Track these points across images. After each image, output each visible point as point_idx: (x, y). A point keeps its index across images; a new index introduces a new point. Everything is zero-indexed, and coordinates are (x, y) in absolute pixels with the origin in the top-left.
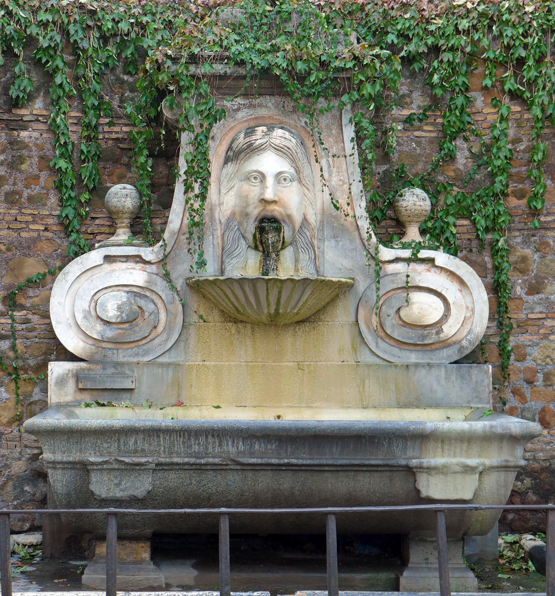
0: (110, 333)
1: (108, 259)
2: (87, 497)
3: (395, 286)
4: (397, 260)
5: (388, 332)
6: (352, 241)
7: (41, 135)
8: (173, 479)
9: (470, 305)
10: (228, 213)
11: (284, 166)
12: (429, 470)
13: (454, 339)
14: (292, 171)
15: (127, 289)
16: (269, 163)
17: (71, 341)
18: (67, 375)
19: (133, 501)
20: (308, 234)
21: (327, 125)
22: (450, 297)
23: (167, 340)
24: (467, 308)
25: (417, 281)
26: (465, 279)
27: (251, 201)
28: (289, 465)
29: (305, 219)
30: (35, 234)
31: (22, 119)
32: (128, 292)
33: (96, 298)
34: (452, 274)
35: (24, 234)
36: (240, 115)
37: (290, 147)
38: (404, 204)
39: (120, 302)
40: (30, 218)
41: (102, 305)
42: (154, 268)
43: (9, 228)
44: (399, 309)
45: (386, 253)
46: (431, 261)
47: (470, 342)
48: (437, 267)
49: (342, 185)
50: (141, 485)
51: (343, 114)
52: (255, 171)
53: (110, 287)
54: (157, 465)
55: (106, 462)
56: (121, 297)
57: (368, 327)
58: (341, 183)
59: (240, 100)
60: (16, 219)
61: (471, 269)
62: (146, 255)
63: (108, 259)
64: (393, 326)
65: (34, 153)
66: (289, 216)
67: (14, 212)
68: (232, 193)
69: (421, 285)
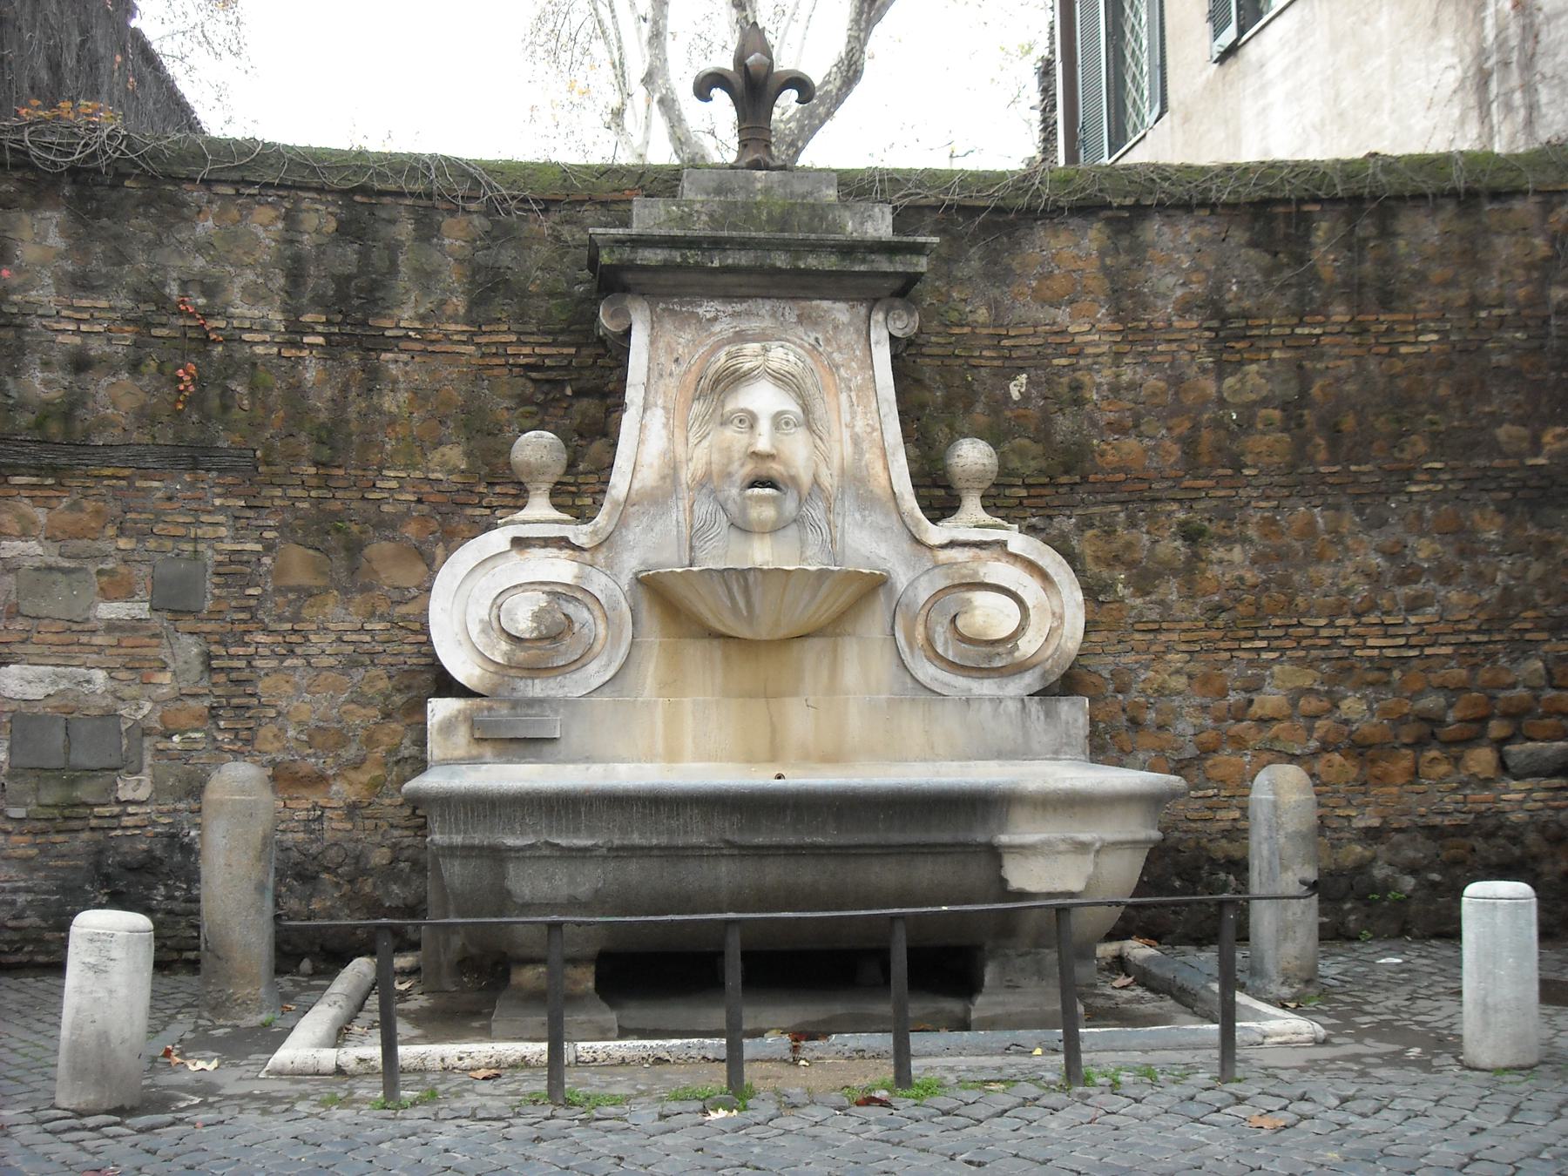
0: (521, 655)
1: (519, 543)
2: (503, 900)
3: (948, 583)
4: (952, 544)
5: (940, 650)
6: (887, 515)
8: (634, 871)
9: (1057, 610)
11: (788, 404)
12: (1021, 849)
13: (1035, 660)
14: (797, 410)
15: (547, 588)
16: (763, 399)
17: (462, 668)
19: (573, 904)
21: (848, 344)
22: (1030, 597)
24: (1054, 614)
26: (1051, 571)
27: (736, 456)
28: (814, 846)
29: (816, 481)
30: (403, 508)
32: (549, 593)
33: (499, 601)
34: (1032, 567)
36: (717, 328)
38: (961, 462)
39: (536, 608)
40: (394, 484)
41: (509, 612)
42: (587, 555)
43: (363, 498)
45: (936, 534)
46: (1003, 544)
50: (587, 880)
52: (742, 410)
54: (609, 849)
55: (531, 846)
62: (576, 536)
63: (519, 543)
64: (946, 643)
66: (794, 480)
68: (705, 443)
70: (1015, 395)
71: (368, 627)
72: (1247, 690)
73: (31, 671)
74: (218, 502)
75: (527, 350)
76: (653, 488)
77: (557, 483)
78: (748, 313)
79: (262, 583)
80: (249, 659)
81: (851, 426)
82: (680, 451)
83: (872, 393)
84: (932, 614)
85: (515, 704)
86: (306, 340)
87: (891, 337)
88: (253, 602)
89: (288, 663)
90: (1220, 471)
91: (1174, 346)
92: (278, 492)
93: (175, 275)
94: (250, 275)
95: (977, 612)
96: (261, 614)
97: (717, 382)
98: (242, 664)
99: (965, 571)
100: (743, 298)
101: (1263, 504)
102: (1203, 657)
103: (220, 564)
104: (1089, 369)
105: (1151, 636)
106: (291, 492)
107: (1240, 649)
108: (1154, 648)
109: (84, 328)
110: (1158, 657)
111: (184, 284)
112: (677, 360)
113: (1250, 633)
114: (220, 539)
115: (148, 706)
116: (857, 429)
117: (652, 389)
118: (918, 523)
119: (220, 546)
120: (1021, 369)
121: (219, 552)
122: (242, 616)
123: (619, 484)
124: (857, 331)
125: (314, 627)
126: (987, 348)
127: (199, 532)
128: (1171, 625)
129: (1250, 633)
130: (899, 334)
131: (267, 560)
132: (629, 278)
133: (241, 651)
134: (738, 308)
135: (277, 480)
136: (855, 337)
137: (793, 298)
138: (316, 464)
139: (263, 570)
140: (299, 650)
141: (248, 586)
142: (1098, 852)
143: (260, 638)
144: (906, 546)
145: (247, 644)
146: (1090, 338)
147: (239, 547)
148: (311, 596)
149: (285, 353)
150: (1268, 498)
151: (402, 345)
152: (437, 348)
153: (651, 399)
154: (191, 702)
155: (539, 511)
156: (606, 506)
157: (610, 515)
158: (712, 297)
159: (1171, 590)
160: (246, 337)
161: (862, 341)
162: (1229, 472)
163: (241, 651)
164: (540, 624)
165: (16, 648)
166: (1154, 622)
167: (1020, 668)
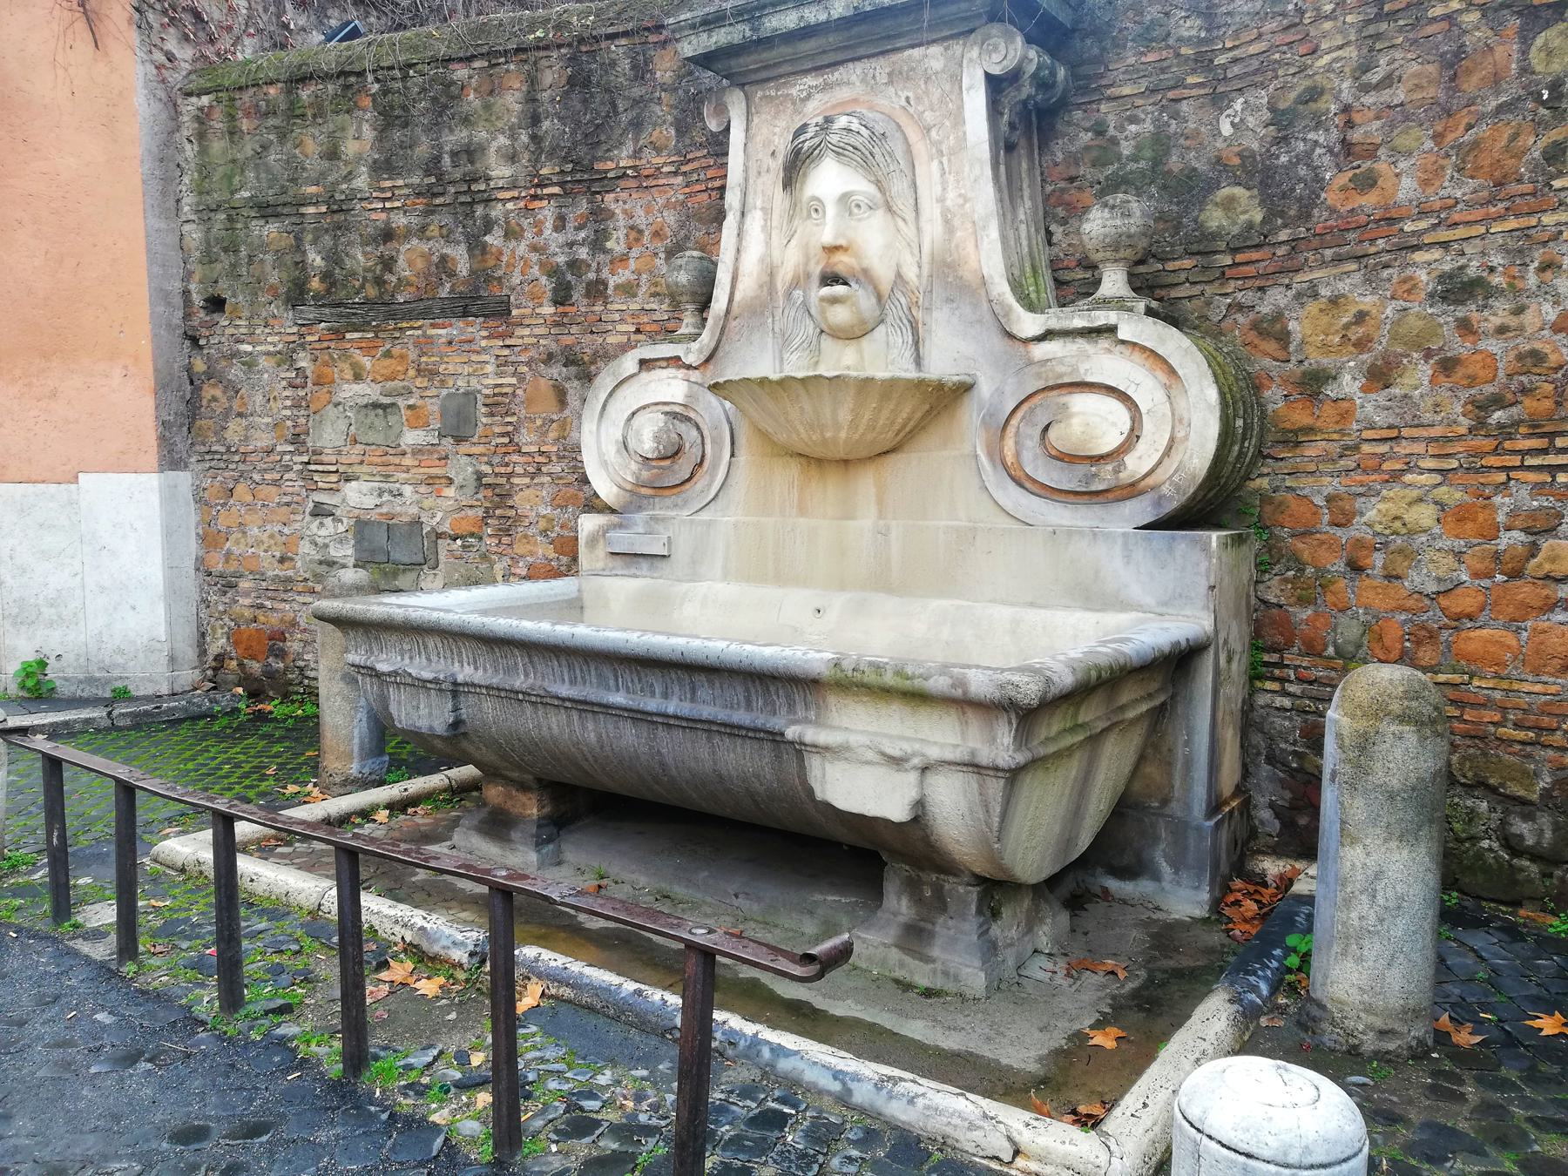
0: (645, 474)
4: (1048, 335)
6: (976, 306)
10: (789, 277)
13: (1150, 481)
14: (871, 189)
17: (604, 487)
20: (903, 300)
23: (710, 485)
29: (899, 275)
30: (624, 339)
32: (666, 413)
37: (857, 144)
40: (617, 317)
42: (695, 376)
43: (592, 332)
45: (1029, 324)
46: (1111, 330)
47: (1178, 488)
48: (1123, 342)
58: (961, 201)
59: (810, 81)
64: (1036, 457)
65: (621, 223)
66: (865, 271)
67: (598, 308)
69: (1089, 379)
70: (1226, 129)
73: (366, 487)
74: (484, 343)
76: (752, 298)
78: (839, 84)
80: (510, 475)
81: (941, 200)
82: (776, 254)
86: (546, 191)
87: (988, 76)
88: (510, 428)
90: (1514, 188)
92: (527, 332)
94: (502, 140)
95: (1075, 421)
99: (1061, 369)
100: (835, 65)
102: (1459, 477)
103: (487, 396)
106: (537, 331)
107: (1522, 467)
109: (388, 205)
114: (486, 375)
115: (439, 515)
116: (949, 203)
118: (1008, 312)
119: (486, 381)
121: (486, 387)
128: (1415, 432)
130: (996, 70)
135: (527, 322)
137: (883, 53)
138: (556, 303)
139: (517, 400)
140: (544, 469)
142: (924, 769)
143: (515, 458)
144: (998, 342)
145: (507, 465)
147: (500, 381)
151: (622, 183)
153: (750, 199)
154: (470, 512)
157: (713, 334)
160: (501, 195)
163: (503, 470)
165: (356, 469)
167: (1131, 490)
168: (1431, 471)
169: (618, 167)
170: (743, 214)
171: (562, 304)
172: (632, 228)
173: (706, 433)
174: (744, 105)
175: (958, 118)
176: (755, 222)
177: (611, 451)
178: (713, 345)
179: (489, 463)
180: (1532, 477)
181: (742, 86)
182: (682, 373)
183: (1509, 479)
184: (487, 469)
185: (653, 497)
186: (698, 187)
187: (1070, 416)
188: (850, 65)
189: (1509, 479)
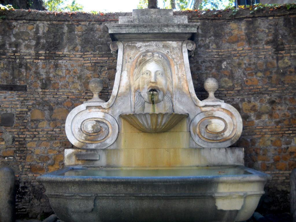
0: (89, 138)
3: (205, 116)
4: (206, 106)
7: (67, 61)
16: (152, 67)
17: (73, 141)
18: (72, 154)
24: (234, 125)
25: (214, 114)
26: (233, 113)
31: (59, 56)
32: (96, 121)
35: (59, 100)
36: (141, 49)
39: (93, 125)
40: (61, 93)
41: (86, 126)
42: (106, 111)
43: (53, 97)
44: (207, 126)
45: (202, 103)
46: (220, 105)
49: (183, 76)
51: (183, 48)
52: (147, 71)
53: (89, 119)
56: (93, 123)
57: (194, 133)
60: (56, 94)
61: (235, 109)
62: (103, 106)
69: (216, 116)
70: (223, 67)
71: (55, 130)
72: (287, 144)
74: (17, 99)
75: (96, 59)
77: (101, 92)
78: (149, 45)
79: (28, 119)
80: (24, 138)
81: (177, 75)
82: (132, 82)
83: (183, 66)
84: (201, 125)
85: (87, 150)
86: (40, 58)
88: (25, 124)
89: (34, 139)
90: (279, 86)
91: (265, 53)
93: (8, 43)
95: (213, 125)
96: (27, 127)
97: (140, 63)
98: (23, 139)
99: (209, 113)
101: (290, 94)
103: (17, 114)
104: (242, 60)
105: (260, 130)
108: (262, 133)
110: (263, 136)
111: (10, 45)
112: (130, 58)
113: (287, 129)
114: (17, 108)
117: (124, 66)
118: (196, 100)
120: (225, 60)
122: (23, 127)
123: (115, 92)
124: (179, 49)
125: (41, 130)
126: (216, 55)
127: (12, 106)
129: (287, 129)
131: (29, 113)
132: (117, 36)
133: (22, 136)
134: (147, 44)
136: (178, 51)
138: (42, 89)
139: (28, 116)
140: (37, 136)
141: (24, 120)
145: (24, 135)
146: (242, 52)
148: (40, 122)
149: (35, 61)
150: (291, 93)
152: (73, 59)
155: (96, 100)
156: (111, 97)
158: (140, 41)
159: (265, 117)
160: (25, 57)
161: (180, 52)
162: (281, 86)
163: (22, 136)
164: (94, 129)
166: (261, 126)
168: (269, 134)
169: (63, 54)
170: (122, 72)
171: (44, 89)
172: (67, 70)
173: (110, 126)
174: (122, 46)
175: (182, 58)
176: (125, 74)
177: (76, 131)
178: (112, 103)
179: (18, 134)
180: (286, 135)
181: (121, 41)
182: (101, 110)
183: (283, 135)
184: (16, 136)
185: (92, 144)
186: (88, 62)
187: (212, 123)
188: (152, 42)
189: (283, 135)
